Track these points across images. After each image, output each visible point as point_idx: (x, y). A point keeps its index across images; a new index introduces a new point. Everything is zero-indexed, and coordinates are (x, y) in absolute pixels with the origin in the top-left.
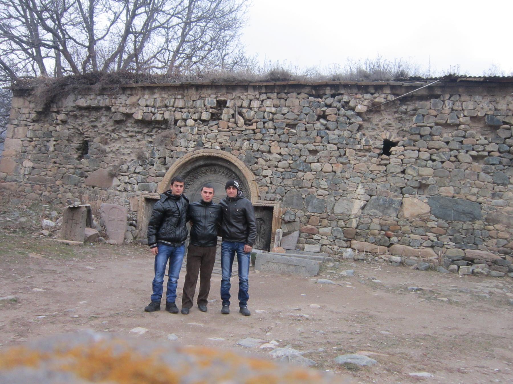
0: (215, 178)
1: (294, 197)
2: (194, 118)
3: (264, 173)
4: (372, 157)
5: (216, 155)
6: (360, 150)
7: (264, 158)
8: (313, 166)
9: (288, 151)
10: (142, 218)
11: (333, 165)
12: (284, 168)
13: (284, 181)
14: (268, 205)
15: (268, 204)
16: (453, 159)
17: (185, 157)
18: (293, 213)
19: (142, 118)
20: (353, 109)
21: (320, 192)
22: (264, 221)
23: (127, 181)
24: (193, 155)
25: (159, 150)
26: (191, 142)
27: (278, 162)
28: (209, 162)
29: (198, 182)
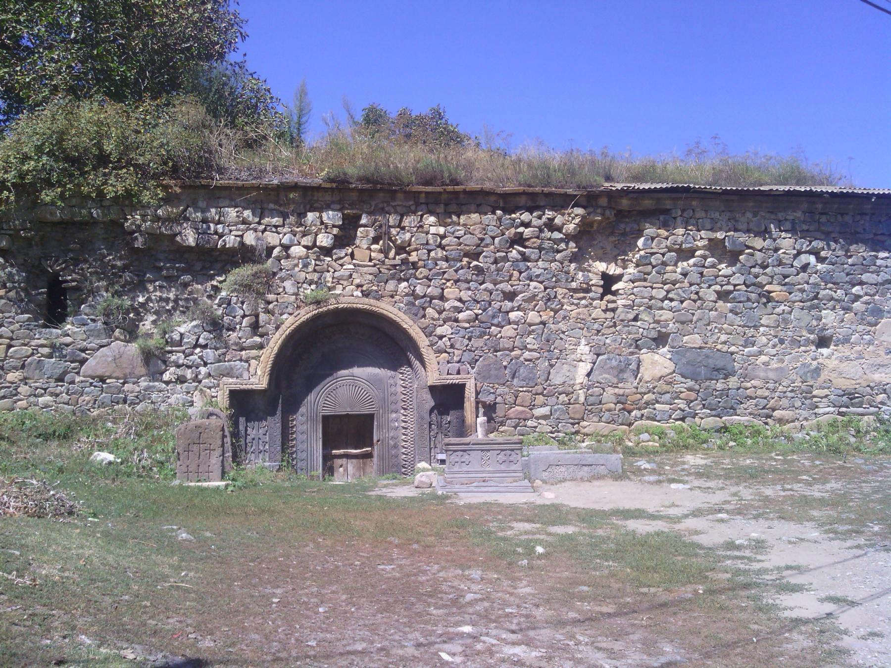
2: (306, 244)
3: (439, 331)
4: (593, 299)
6: (575, 291)
8: (513, 315)
11: (541, 313)
15: (455, 379)
16: (696, 297)
19: (197, 244)
20: (559, 229)
21: (527, 354)
23: (181, 362)
26: (305, 285)
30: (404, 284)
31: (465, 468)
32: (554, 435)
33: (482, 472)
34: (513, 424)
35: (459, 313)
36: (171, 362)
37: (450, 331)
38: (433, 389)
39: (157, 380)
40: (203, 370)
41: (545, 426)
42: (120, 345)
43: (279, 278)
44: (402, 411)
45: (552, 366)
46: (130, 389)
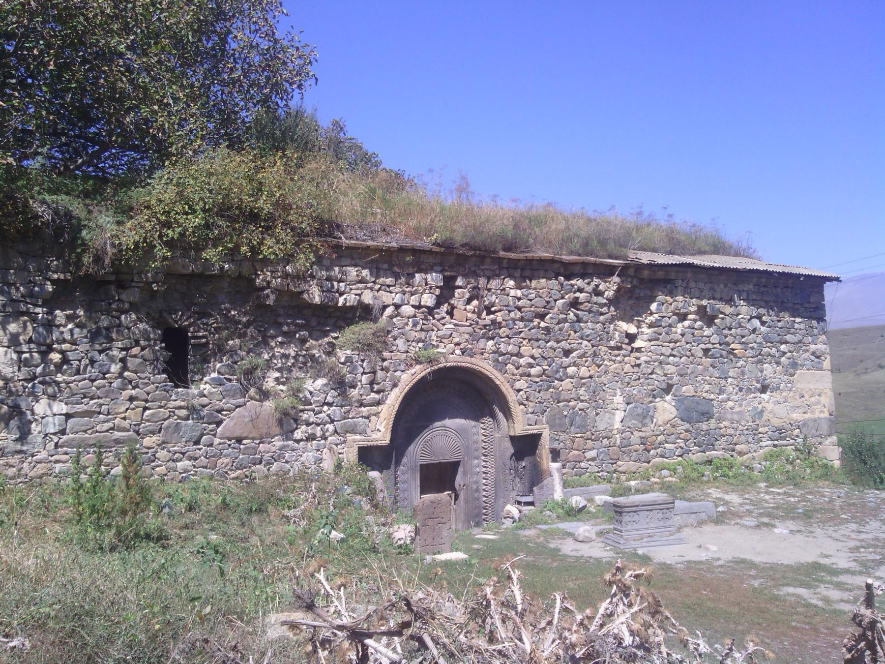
2: (414, 303)
4: (624, 356)
8: (571, 370)
15: (534, 430)
16: (688, 353)
23: (311, 420)
30: (491, 343)
31: (636, 526)
32: (600, 474)
33: (648, 529)
34: (572, 467)
35: (531, 368)
36: (302, 421)
38: (514, 439)
39: (288, 439)
40: (330, 427)
41: (593, 467)
42: (256, 405)
43: (392, 337)
44: (483, 458)
45: (597, 414)
46: (267, 450)
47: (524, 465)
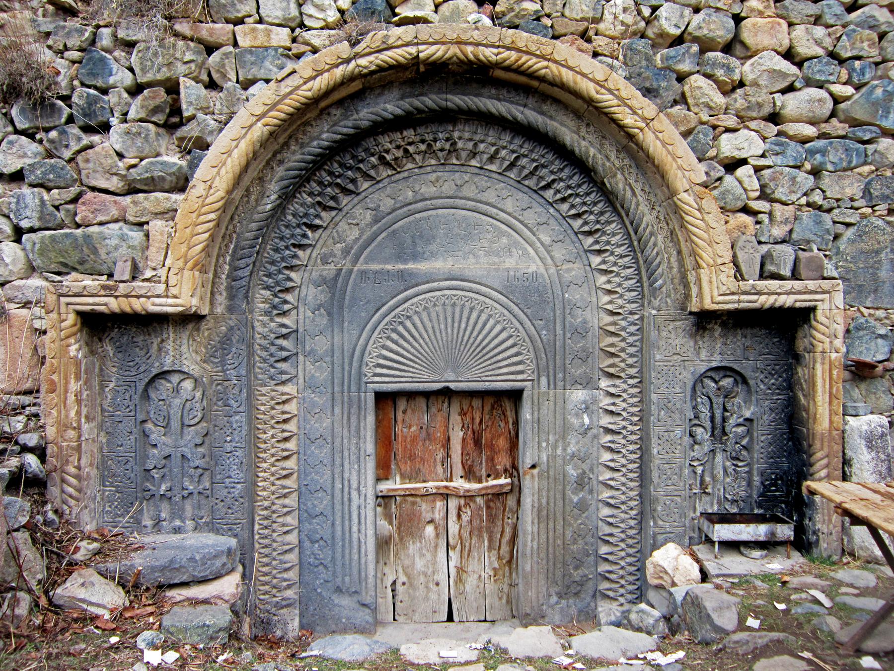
0: (448, 188)
1: (883, 256)
3: (728, 146)
5: (488, 54)
7: (720, 73)
9: (828, 42)
10: (78, 428)
12: (812, 124)
13: (827, 181)
14: (787, 301)
17: (308, 73)
18: (882, 331)
22: (743, 380)
24: (357, 56)
25: (130, 45)
27: (784, 91)
28: (430, 101)
29: (358, 211)
37: (759, 147)
44: (604, 383)
47: (748, 414)
